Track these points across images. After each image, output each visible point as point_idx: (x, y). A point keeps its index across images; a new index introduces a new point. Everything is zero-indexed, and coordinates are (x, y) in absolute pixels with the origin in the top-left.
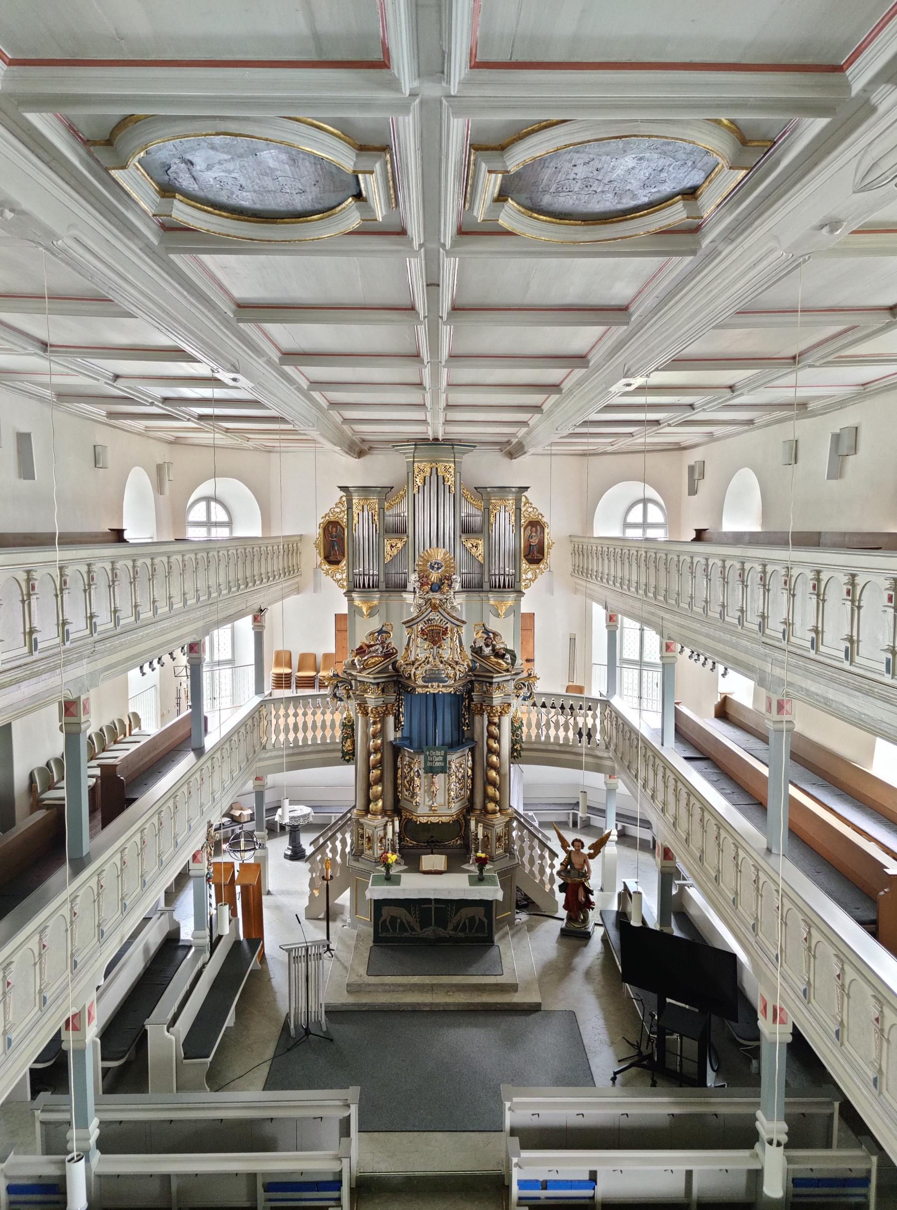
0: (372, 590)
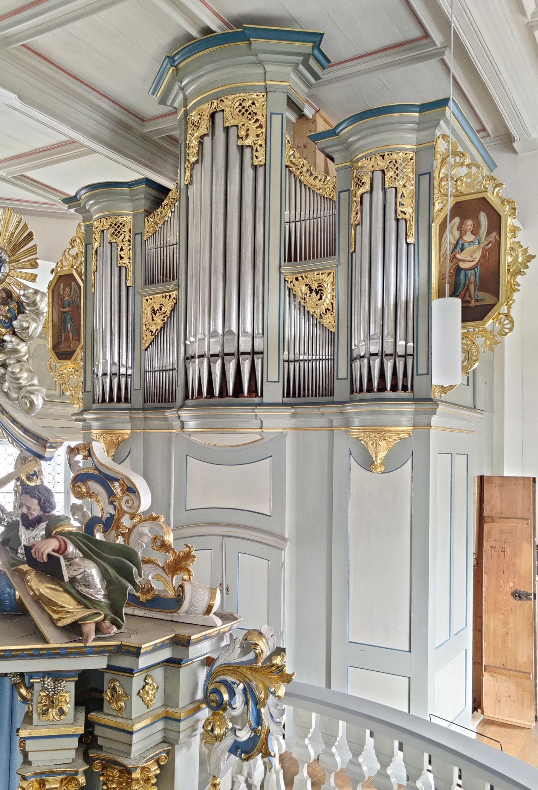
0: (115, 405)
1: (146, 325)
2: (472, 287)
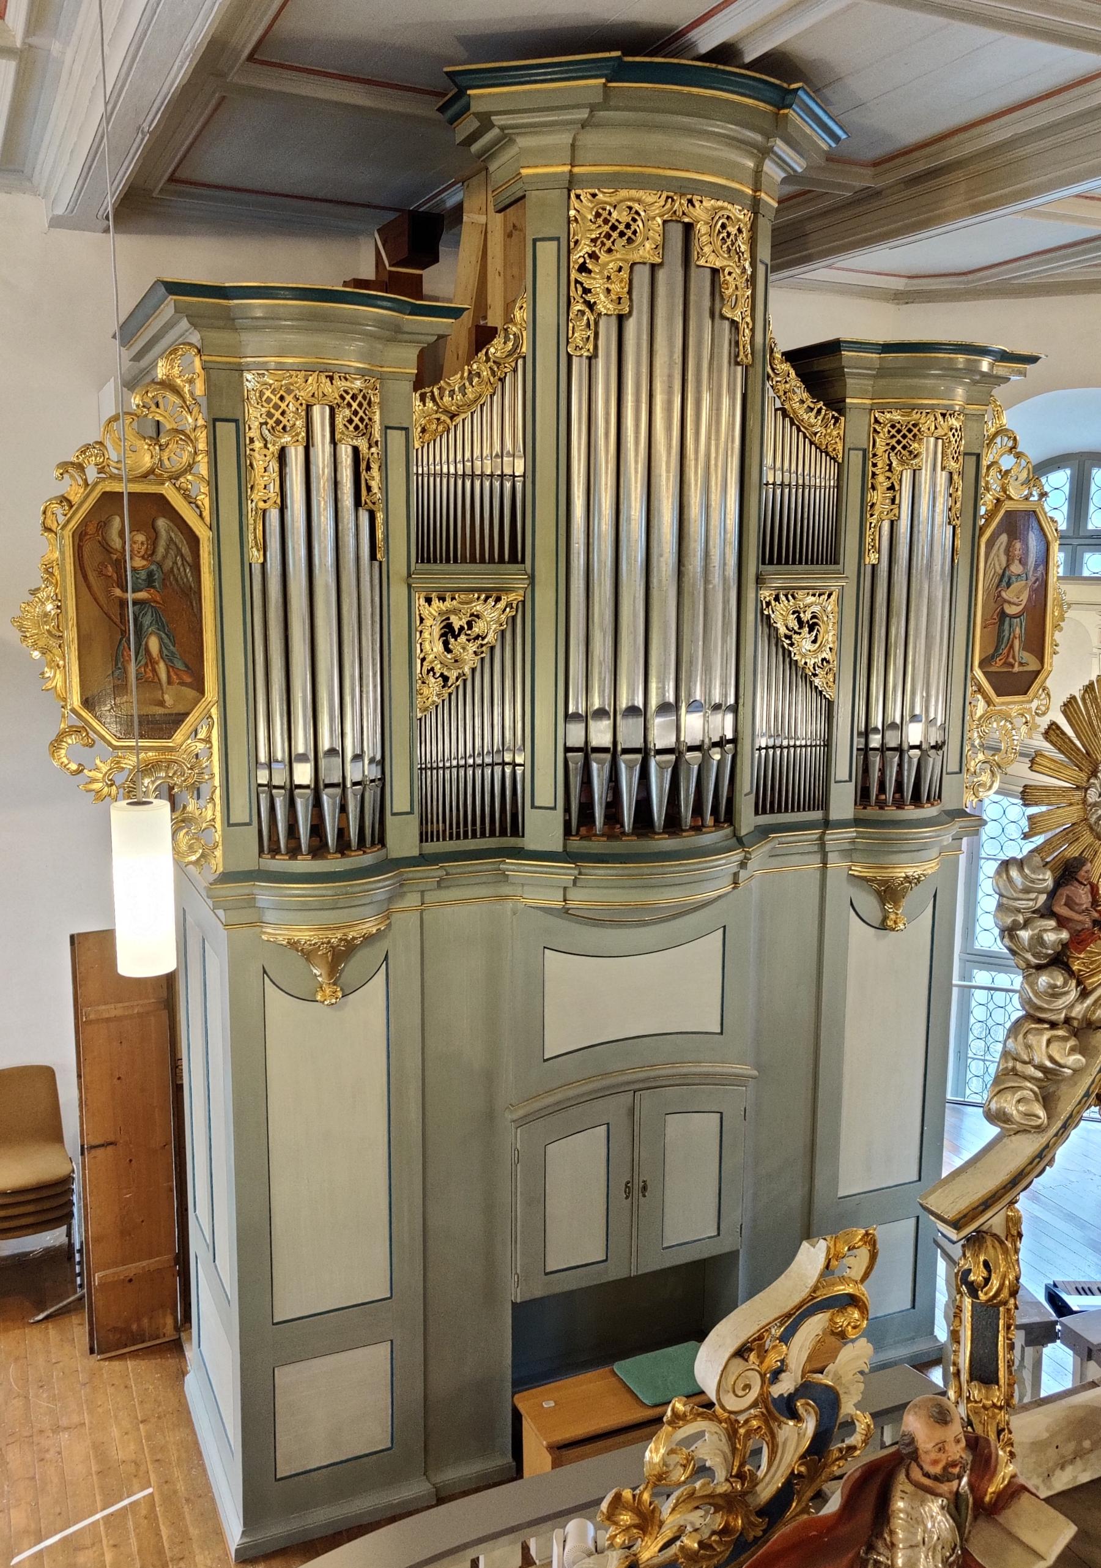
1: (423, 660)
2: (1017, 643)
